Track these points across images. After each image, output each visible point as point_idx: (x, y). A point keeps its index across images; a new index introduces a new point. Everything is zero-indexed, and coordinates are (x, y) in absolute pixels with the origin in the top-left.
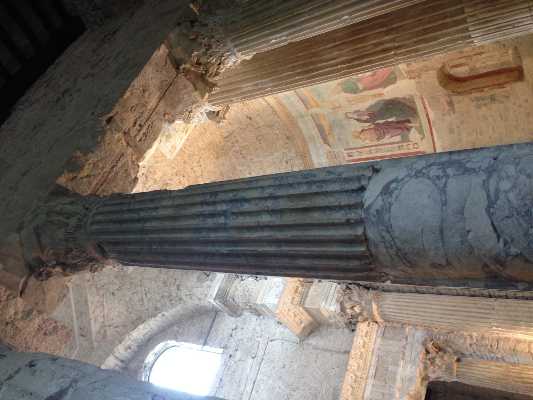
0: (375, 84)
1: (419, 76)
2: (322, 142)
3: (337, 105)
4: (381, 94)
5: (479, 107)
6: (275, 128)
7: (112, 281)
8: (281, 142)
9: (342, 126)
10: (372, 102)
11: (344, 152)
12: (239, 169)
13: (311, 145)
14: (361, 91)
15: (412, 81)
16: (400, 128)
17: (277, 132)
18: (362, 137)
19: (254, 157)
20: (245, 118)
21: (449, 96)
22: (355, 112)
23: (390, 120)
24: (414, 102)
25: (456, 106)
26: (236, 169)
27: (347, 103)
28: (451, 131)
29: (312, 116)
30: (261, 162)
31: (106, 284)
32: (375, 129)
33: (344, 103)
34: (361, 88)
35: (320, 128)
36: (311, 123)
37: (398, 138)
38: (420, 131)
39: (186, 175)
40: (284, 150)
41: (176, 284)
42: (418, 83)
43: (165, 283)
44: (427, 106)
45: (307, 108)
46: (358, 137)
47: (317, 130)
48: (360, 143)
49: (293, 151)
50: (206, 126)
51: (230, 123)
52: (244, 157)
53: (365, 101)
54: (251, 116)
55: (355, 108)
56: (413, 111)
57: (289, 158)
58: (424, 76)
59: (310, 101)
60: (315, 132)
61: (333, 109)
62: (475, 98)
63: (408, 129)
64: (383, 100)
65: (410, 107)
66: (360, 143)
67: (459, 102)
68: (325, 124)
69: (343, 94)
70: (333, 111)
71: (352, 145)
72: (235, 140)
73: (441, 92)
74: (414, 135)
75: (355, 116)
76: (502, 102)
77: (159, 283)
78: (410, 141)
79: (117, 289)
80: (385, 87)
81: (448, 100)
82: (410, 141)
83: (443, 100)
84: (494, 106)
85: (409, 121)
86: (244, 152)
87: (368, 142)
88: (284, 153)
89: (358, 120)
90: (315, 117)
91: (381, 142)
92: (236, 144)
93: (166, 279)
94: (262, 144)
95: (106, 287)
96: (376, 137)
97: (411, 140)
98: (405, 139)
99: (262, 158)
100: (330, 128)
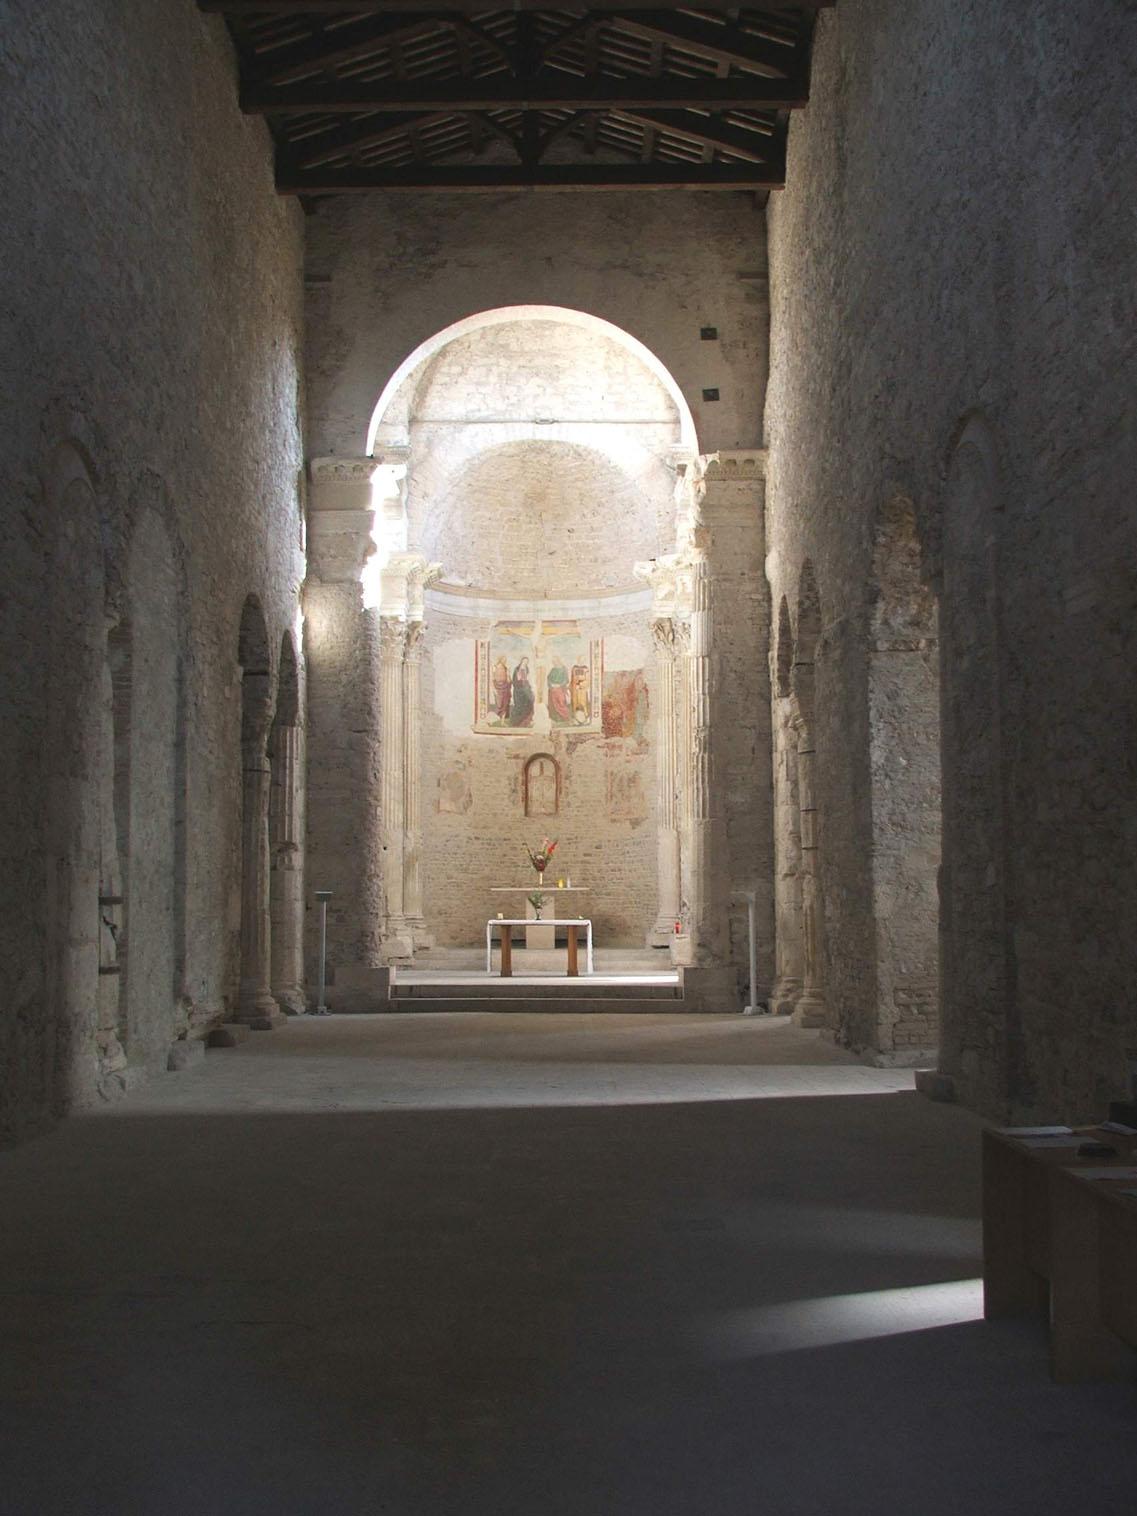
0: (554, 700)
1: (551, 740)
2: (501, 619)
3: (540, 654)
4: (541, 700)
5: (509, 778)
8: (513, 572)
9: (514, 648)
10: (535, 689)
11: (488, 640)
12: (501, 508)
13: (498, 604)
14: (549, 685)
15: (547, 733)
16: (502, 706)
17: (526, 574)
18: (500, 666)
20: (554, 549)
21: (524, 758)
22: (527, 668)
23: (512, 699)
24: (525, 727)
25: (513, 761)
28: (491, 751)
29: (533, 622)
32: (505, 682)
33: (540, 662)
34: (553, 685)
35: (518, 624)
36: (524, 617)
37: (493, 701)
38: (495, 724)
42: (544, 737)
44: (520, 737)
45: (544, 622)
46: (500, 662)
47: (515, 619)
48: (494, 661)
49: (499, 581)
52: (509, 520)
54: (553, 557)
55: (531, 670)
56: (516, 724)
58: (550, 743)
59: (552, 629)
60: (513, 616)
61: (536, 649)
62: (517, 778)
63: (499, 714)
64: (534, 700)
65: (521, 721)
66: (494, 661)
67: (517, 764)
68: (520, 631)
69: (552, 666)
70: (534, 645)
71: (492, 651)
72: (533, 521)
73: (530, 753)
74: (493, 717)
75: (522, 667)
76: (510, 796)
78: (489, 711)
80: (548, 708)
81: (522, 756)
82: (489, 711)
83: (521, 752)
84: (507, 791)
85: (506, 717)
86: (515, 524)
87: (493, 669)
89: (518, 668)
90: (531, 624)
91: (492, 684)
92: (528, 519)
94: (515, 550)
96: (498, 679)
97: (491, 713)
98: (491, 708)
100: (514, 635)
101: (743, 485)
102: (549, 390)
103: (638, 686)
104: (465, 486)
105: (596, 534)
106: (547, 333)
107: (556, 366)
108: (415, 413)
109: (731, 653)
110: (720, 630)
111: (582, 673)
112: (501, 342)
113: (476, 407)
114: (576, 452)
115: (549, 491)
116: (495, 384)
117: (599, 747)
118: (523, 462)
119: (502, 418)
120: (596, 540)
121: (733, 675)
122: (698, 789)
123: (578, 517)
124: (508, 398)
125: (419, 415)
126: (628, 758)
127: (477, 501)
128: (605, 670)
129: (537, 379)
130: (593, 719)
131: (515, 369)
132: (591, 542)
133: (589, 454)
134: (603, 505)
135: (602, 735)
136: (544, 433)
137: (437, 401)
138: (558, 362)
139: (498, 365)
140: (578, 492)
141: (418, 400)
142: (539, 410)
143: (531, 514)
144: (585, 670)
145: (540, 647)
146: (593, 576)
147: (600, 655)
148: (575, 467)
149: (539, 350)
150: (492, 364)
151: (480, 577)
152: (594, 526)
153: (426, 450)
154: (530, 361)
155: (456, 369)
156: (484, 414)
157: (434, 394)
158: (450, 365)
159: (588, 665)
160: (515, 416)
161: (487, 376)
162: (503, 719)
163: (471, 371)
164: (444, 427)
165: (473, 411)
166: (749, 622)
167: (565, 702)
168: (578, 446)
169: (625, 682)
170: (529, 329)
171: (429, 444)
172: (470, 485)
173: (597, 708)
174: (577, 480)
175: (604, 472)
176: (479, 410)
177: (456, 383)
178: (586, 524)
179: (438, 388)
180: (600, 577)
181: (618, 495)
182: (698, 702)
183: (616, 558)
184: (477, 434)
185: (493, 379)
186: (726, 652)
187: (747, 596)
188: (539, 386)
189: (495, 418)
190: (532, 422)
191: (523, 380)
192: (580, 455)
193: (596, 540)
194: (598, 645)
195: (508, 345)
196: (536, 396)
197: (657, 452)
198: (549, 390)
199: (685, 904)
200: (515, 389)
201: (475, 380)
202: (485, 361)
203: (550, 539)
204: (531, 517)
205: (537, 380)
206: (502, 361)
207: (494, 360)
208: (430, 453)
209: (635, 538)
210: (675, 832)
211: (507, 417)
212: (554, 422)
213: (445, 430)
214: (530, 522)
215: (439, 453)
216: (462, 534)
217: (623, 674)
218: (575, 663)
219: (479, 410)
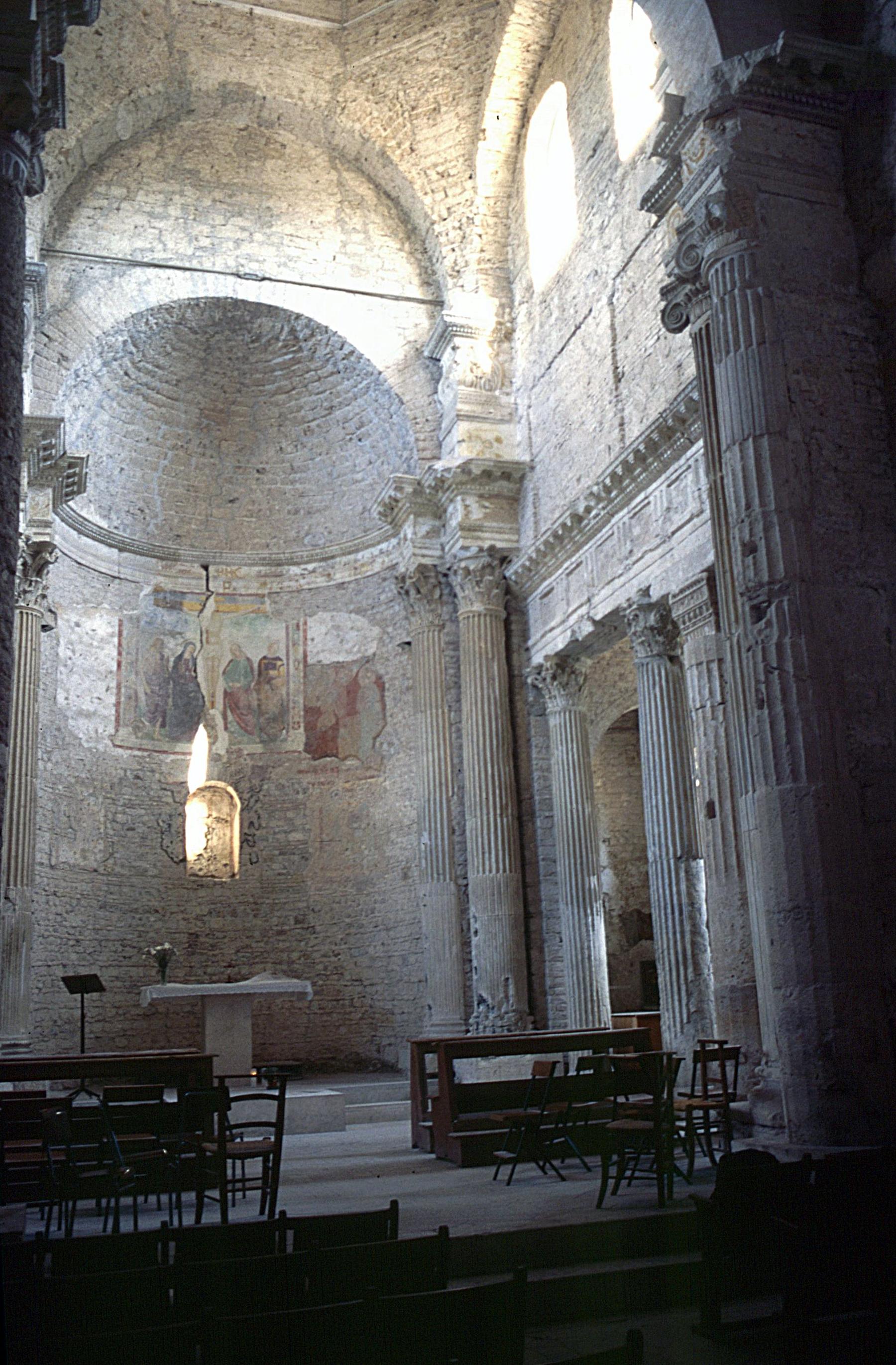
3: (212, 640)
4: (213, 705)
6: (203, 527)
7: (119, 56)
12: (163, 427)
17: (193, 527)
19: (166, 462)
20: (236, 495)
26: (166, 423)
27: (211, 655)
30: (156, 470)
31: (122, 36)
39: (227, 362)
40: (161, 517)
41: (55, 176)
43: (67, 153)
49: (156, 532)
50: (260, 436)
51: (239, 467)
52: (174, 447)
53: (207, 680)
54: (236, 505)
57: (148, 518)
75: (187, 656)
77: (73, 142)
79: (100, 49)
85: (163, 725)
86: (181, 453)
88: (156, 516)
93: (70, 160)
94: (181, 490)
95: (117, 31)
99: (160, 474)
101: (804, 128)
102: (258, 237)
103: (366, 681)
104: (122, 373)
105: (298, 475)
106: (255, 164)
107: (268, 208)
108: (50, 241)
109: (822, 431)
110: (799, 383)
111: (274, 667)
112: (188, 166)
113: (149, 246)
114: (293, 331)
115: (233, 408)
116: (177, 219)
117: (300, 772)
118: (208, 349)
119: (187, 265)
120: (298, 486)
121: (831, 475)
122: (787, 715)
123: (272, 452)
124: (196, 239)
125: (59, 246)
126: (347, 785)
127: (132, 406)
128: (310, 661)
129: (240, 219)
130: (291, 731)
131: (207, 202)
132: (290, 487)
133: (312, 335)
134: (313, 432)
135: (304, 755)
136: (249, 292)
137: (87, 230)
138: (271, 204)
139: (182, 194)
140: (276, 411)
141: (56, 224)
142: (243, 261)
143: (206, 442)
144: (279, 663)
145: (211, 629)
146: (293, 534)
147: (301, 643)
148: (283, 366)
149: (243, 184)
150: (173, 193)
151: (129, 520)
152: (295, 464)
153: (67, 295)
154: (230, 196)
155: (117, 191)
156: (159, 256)
157: (83, 220)
158: (109, 184)
159: (284, 658)
160: (207, 265)
161: (166, 206)
162: (157, 729)
163: (141, 197)
164: (97, 267)
165: (142, 250)
166: (847, 377)
167: (249, 707)
168: (298, 316)
169: (344, 678)
170: (230, 154)
171: (71, 287)
172: (126, 374)
173: (297, 714)
174: (279, 391)
175: (330, 368)
176: (152, 250)
177: (118, 209)
178: (283, 462)
179: (91, 213)
180: (302, 534)
181: (338, 414)
182: (767, 529)
183: (327, 508)
184: (148, 281)
185: (174, 211)
186: (814, 429)
187: (838, 328)
188: (243, 229)
189: (170, 263)
190: (232, 274)
191: (219, 220)
192: (296, 338)
193: (298, 486)
194: (298, 626)
195: (199, 172)
196: (238, 243)
197: (412, 338)
198: (258, 237)
199: (482, 1001)
200: (206, 230)
201: (147, 209)
202: (163, 186)
203: (230, 481)
204: (205, 446)
205: (240, 221)
206: (189, 191)
207: (177, 188)
208: (72, 299)
209: (359, 476)
210: (452, 887)
211: (195, 264)
212: (264, 279)
213: (97, 271)
214: (204, 455)
215: (87, 302)
216: (107, 451)
217: (338, 666)
218: (265, 653)
219: (152, 250)
